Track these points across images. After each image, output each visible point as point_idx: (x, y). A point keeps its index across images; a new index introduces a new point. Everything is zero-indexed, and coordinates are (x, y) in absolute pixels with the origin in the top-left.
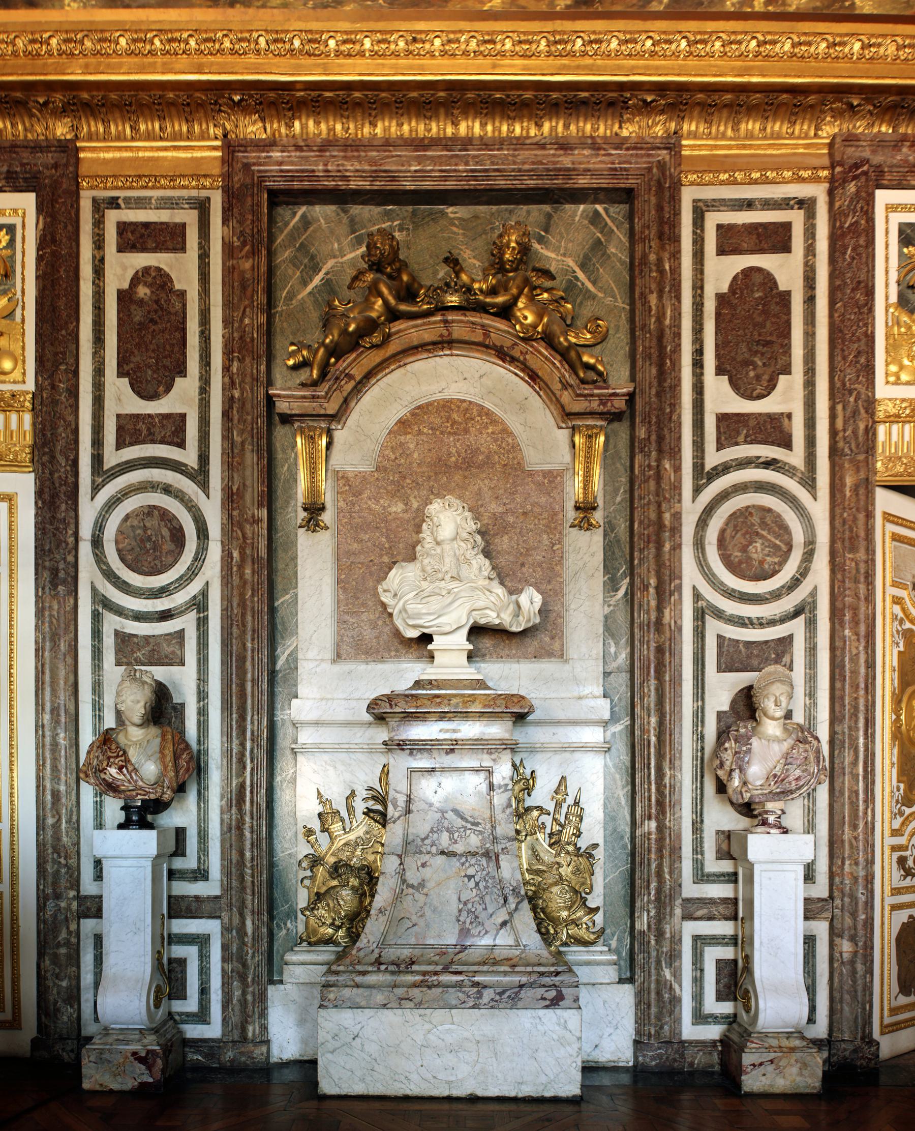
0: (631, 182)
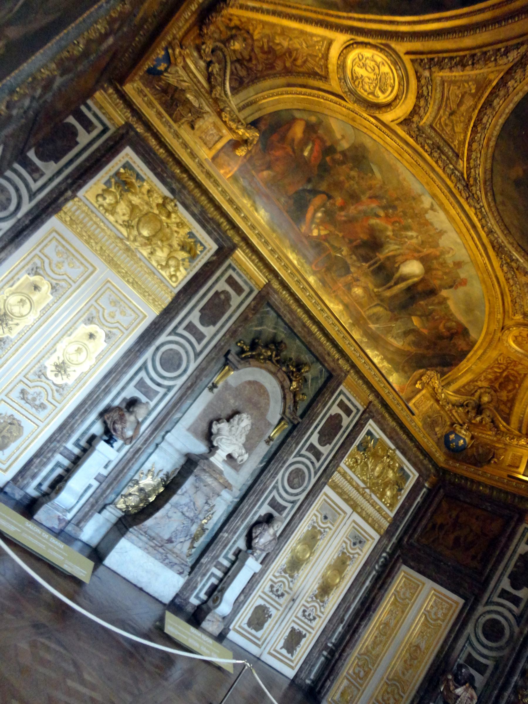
0: (334, 374)
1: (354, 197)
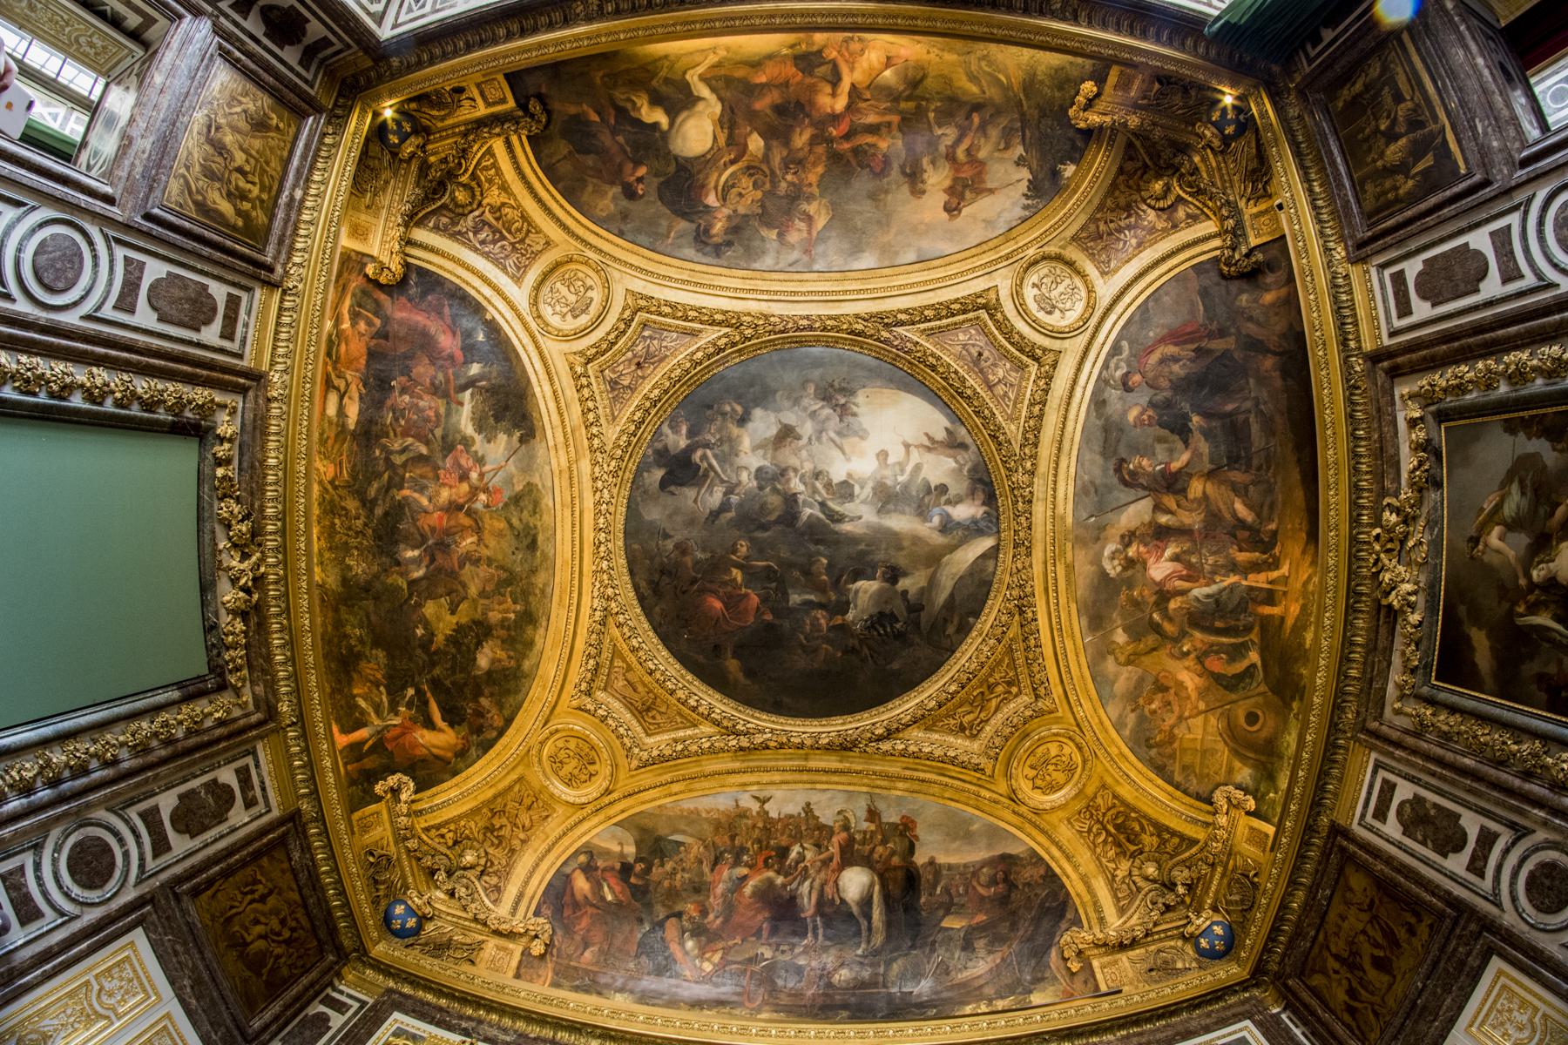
1: (699, 888)
